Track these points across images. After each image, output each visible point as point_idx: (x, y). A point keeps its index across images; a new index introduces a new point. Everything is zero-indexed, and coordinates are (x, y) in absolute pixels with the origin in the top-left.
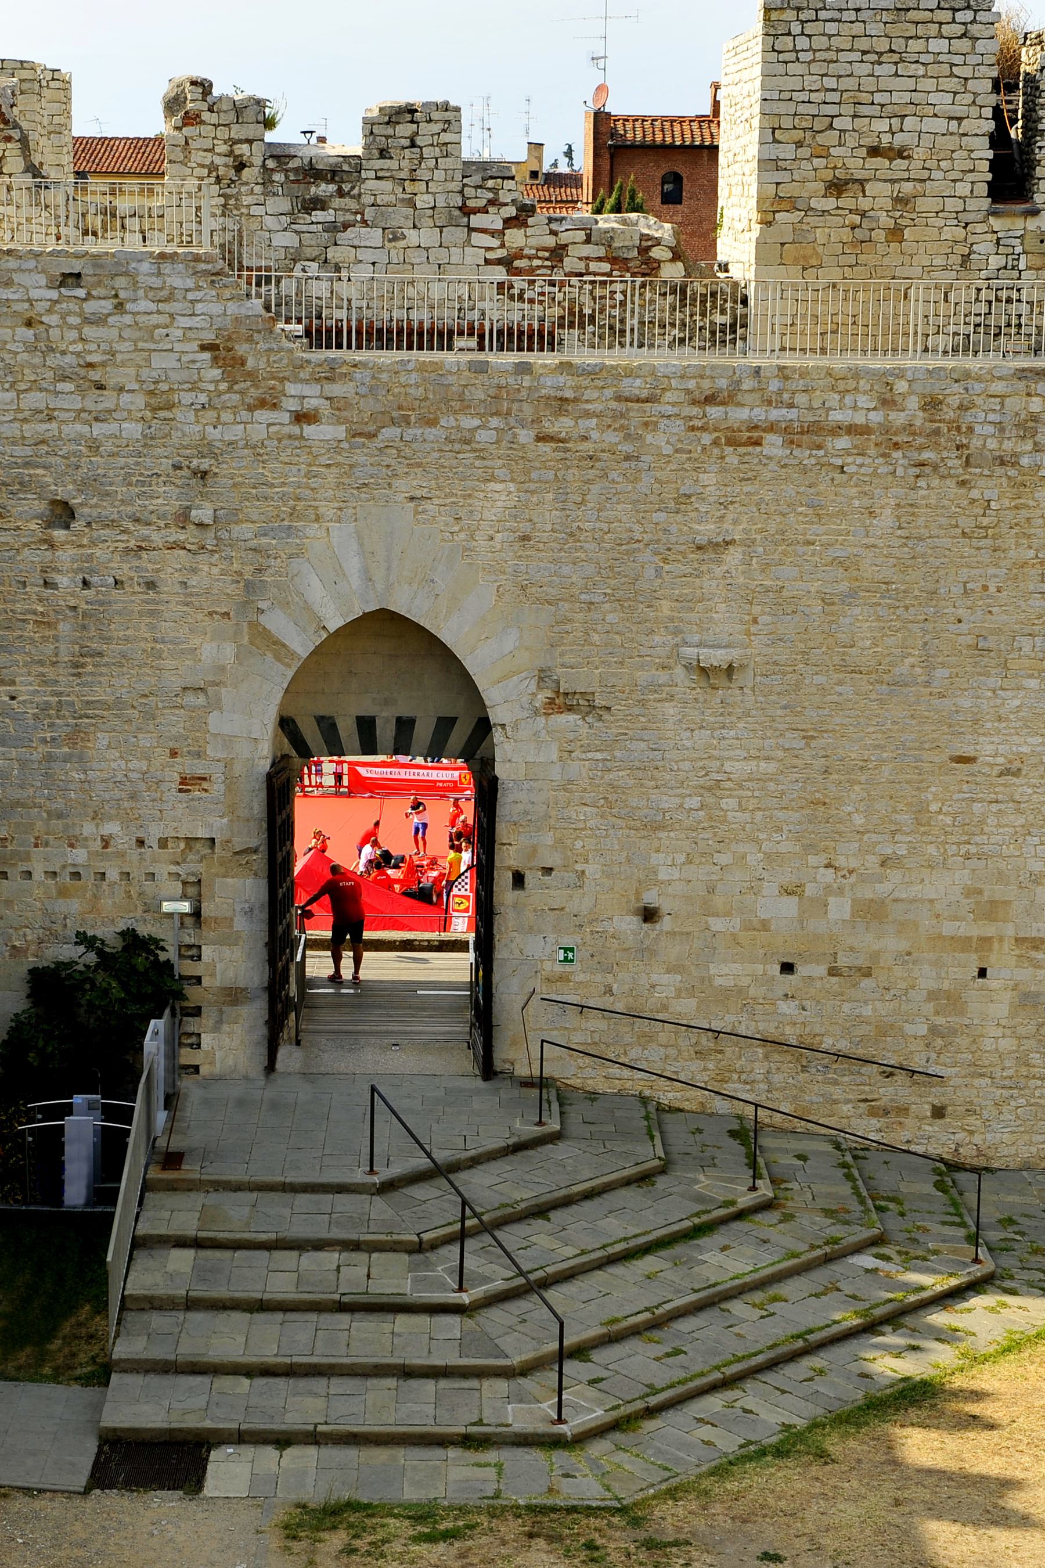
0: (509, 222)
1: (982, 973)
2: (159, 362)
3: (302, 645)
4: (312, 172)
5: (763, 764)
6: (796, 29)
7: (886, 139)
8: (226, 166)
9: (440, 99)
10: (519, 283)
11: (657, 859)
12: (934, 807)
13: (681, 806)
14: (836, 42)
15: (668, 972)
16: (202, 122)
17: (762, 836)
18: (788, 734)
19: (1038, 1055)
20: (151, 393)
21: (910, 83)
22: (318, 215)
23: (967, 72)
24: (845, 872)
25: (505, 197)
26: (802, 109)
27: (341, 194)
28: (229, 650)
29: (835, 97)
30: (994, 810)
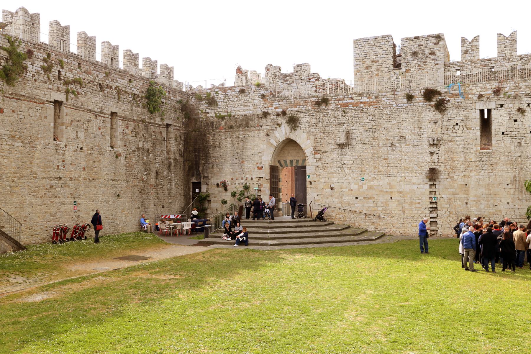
0: (316, 80)
4: (286, 76)
7: (375, 59)
10: (318, 90)
11: (333, 179)
12: (381, 168)
22: (287, 82)
25: (315, 76)
27: (290, 78)
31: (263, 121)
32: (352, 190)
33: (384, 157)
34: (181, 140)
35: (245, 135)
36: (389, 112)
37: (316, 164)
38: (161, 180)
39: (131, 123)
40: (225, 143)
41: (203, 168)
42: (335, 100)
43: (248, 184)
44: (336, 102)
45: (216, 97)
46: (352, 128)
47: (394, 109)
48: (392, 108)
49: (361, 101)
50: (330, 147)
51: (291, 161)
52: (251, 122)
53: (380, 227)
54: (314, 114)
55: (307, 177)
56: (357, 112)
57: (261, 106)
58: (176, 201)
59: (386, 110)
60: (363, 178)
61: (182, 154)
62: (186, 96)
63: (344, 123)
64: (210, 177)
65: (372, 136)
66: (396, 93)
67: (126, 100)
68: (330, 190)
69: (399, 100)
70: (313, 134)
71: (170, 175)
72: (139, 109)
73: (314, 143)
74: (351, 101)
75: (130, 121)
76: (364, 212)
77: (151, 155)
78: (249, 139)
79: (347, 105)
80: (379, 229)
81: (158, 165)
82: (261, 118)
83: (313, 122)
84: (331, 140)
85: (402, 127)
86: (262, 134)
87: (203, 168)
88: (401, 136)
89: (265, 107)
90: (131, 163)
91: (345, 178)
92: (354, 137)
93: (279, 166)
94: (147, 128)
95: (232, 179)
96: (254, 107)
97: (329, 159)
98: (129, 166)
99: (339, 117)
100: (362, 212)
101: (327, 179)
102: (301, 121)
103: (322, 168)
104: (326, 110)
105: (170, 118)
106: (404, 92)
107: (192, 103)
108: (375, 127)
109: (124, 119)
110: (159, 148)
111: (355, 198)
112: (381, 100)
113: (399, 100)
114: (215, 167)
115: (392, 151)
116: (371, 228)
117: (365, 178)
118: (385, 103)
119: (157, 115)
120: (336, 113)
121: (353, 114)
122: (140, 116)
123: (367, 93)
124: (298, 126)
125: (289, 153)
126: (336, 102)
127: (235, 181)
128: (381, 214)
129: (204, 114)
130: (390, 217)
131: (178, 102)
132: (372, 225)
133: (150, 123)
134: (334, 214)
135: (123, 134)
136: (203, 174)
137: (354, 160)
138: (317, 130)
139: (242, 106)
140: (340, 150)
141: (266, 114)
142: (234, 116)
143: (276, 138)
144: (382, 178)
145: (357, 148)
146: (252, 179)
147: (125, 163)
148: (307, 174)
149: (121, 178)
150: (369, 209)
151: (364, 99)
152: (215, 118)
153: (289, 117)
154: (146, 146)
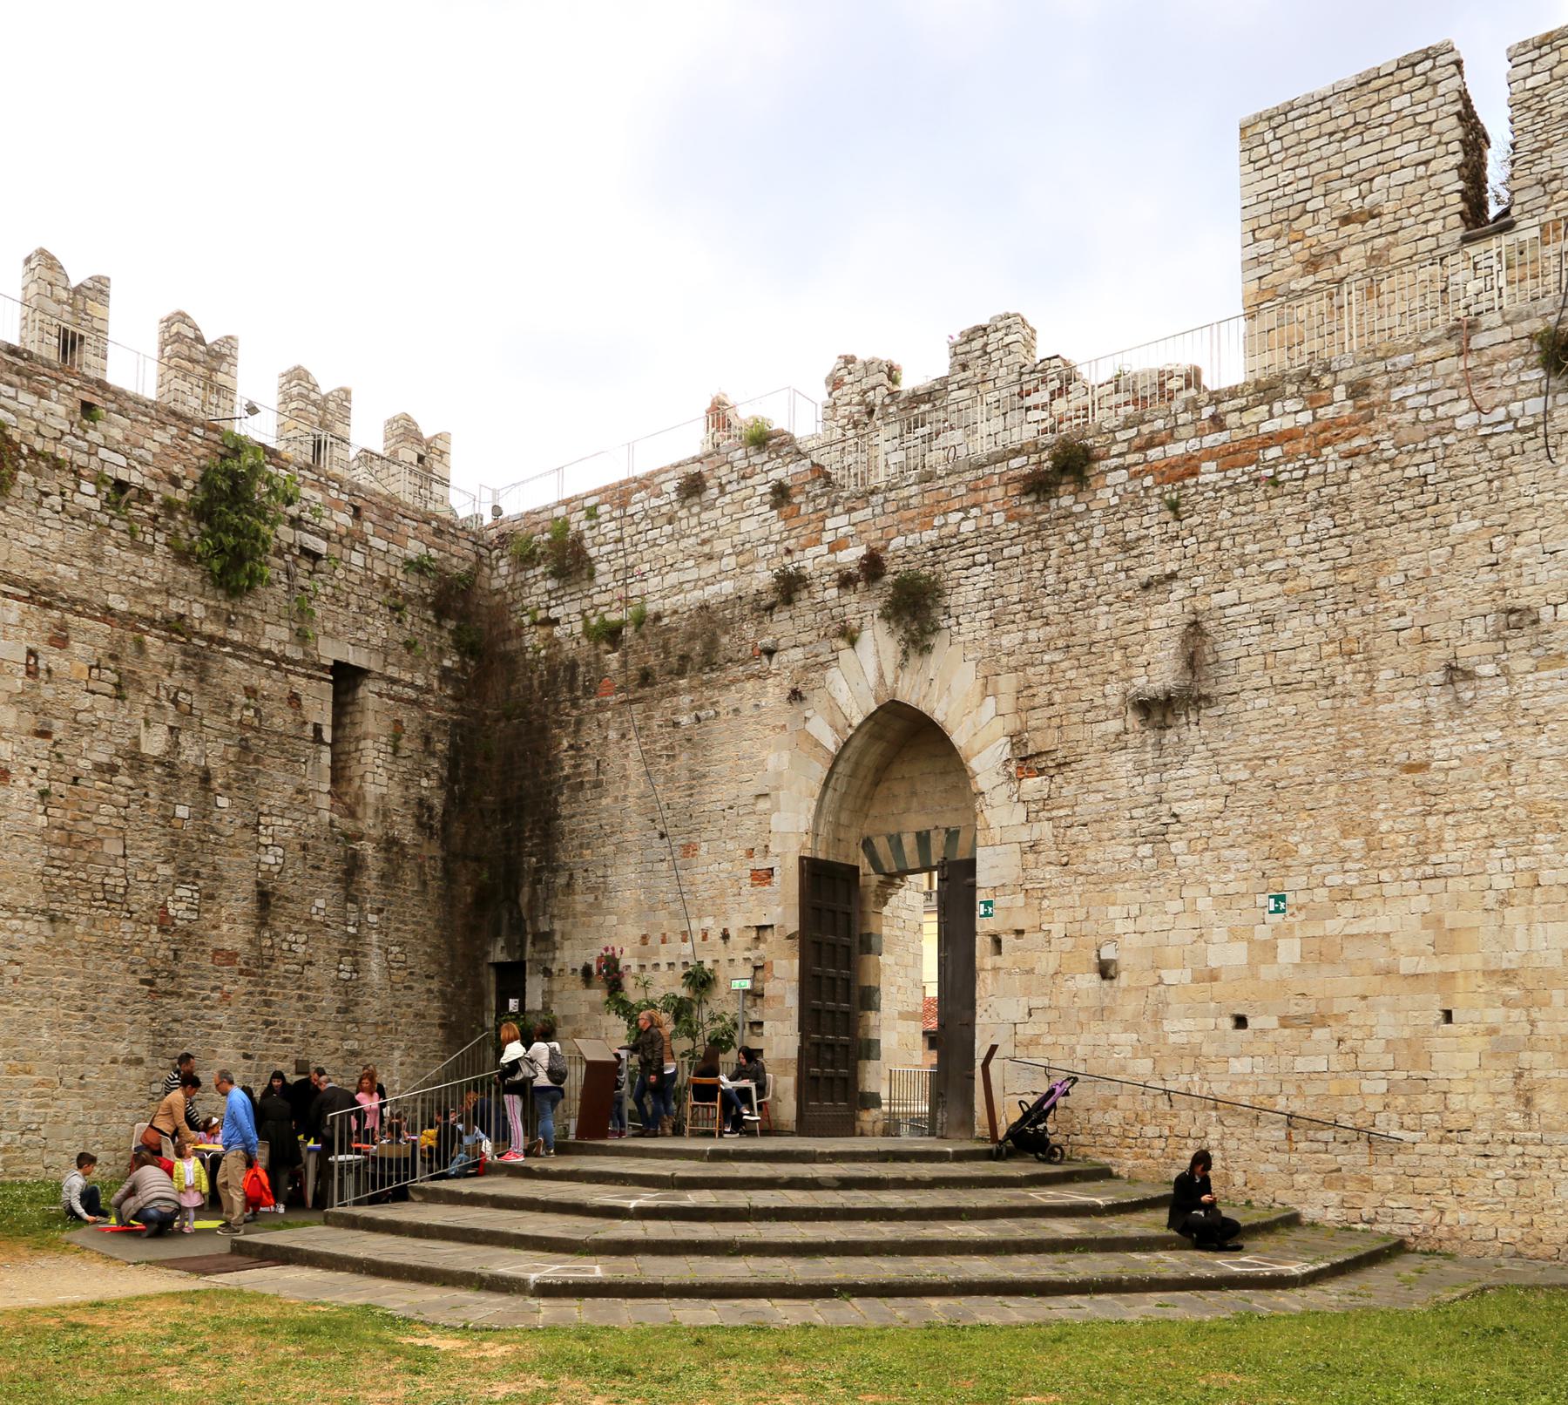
1: (1448, 1016)
3: (831, 742)
5: (1209, 801)
6: (1269, 136)
8: (859, 412)
9: (1002, 312)
11: (1114, 911)
12: (1384, 827)
13: (1135, 855)
14: (1305, 135)
15: (1126, 1031)
16: (844, 384)
17: (1211, 878)
18: (1233, 767)
20: (741, 553)
21: (1376, 146)
23: (1430, 116)
24: (1294, 909)
26: (1277, 204)
28: (786, 756)
29: (1307, 182)
30: (1451, 822)
31: (781, 626)
32: (1213, 977)
33: (1401, 757)
34: (433, 754)
35: (701, 707)
36: (1431, 468)
37: (1025, 835)
38: (291, 937)
39: (90, 623)
40: (619, 762)
41: (534, 891)
42: (1123, 447)
43: (708, 965)
44: (1131, 458)
45: (587, 534)
46: (1217, 599)
48: (1449, 439)
49: (1267, 427)
50: (1099, 729)
51: (923, 839)
52: (725, 640)
53: (1373, 1198)
54: (1017, 550)
55: (981, 909)
56: (1244, 496)
57: (772, 547)
58: (392, 1048)
59: (1418, 458)
60: (1280, 898)
61: (437, 824)
62: (469, 545)
63: (1172, 576)
64: (557, 938)
65: (1335, 632)
66: (1479, 341)
67: (56, 500)
68: (1096, 977)
69: (1496, 382)
71: (353, 917)
72: (147, 561)
73: (1018, 711)
74: (1208, 441)
75: (78, 614)
76: (1281, 1103)
77: (223, 802)
78: (718, 727)
79: (1188, 467)
80: (1367, 1213)
81: (271, 860)
82: (770, 608)
83: (1014, 591)
84: (1105, 682)
85: (1517, 552)
86: (773, 693)
87: (534, 891)
88: (1512, 611)
89: (789, 552)
90: (85, 826)
91: (1175, 906)
92: (1231, 649)
93: (864, 864)
94: (198, 664)
96: (741, 559)
97: (1093, 798)
98: (68, 842)
99: (1145, 546)
100: (1267, 1103)
101: (1081, 914)
102: (946, 601)
103: (1053, 855)
104: (1078, 516)
105: (360, 635)
106: (1525, 327)
107: (497, 584)
108: (1352, 574)
110: (280, 776)
111: (1228, 1023)
112: (1384, 405)
113: (1496, 382)
114: (579, 882)
115: (1452, 716)
116: (1321, 1206)
117: (1290, 897)
118: (1409, 416)
119: (271, 608)
120: (1130, 524)
121: (1224, 514)
122: (157, 600)
123: (1305, 376)
124: (937, 629)
125: (914, 794)
126: (1131, 458)
127: (657, 954)
128: (1381, 1120)
129: (543, 632)
130: (1435, 1135)
132: (1327, 1184)
133: (223, 642)
134: (1113, 1118)
135: (32, 672)
136: (534, 920)
137: (1226, 789)
138: (1032, 636)
139: (691, 563)
140: (1151, 736)
141: (790, 586)
142: (658, 617)
143: (834, 706)
144: (1391, 890)
145: (1246, 717)
146: (725, 936)
147: (41, 821)
148: (981, 896)
150: (1309, 1089)
151: (1289, 415)
152: (584, 642)
154: (190, 753)
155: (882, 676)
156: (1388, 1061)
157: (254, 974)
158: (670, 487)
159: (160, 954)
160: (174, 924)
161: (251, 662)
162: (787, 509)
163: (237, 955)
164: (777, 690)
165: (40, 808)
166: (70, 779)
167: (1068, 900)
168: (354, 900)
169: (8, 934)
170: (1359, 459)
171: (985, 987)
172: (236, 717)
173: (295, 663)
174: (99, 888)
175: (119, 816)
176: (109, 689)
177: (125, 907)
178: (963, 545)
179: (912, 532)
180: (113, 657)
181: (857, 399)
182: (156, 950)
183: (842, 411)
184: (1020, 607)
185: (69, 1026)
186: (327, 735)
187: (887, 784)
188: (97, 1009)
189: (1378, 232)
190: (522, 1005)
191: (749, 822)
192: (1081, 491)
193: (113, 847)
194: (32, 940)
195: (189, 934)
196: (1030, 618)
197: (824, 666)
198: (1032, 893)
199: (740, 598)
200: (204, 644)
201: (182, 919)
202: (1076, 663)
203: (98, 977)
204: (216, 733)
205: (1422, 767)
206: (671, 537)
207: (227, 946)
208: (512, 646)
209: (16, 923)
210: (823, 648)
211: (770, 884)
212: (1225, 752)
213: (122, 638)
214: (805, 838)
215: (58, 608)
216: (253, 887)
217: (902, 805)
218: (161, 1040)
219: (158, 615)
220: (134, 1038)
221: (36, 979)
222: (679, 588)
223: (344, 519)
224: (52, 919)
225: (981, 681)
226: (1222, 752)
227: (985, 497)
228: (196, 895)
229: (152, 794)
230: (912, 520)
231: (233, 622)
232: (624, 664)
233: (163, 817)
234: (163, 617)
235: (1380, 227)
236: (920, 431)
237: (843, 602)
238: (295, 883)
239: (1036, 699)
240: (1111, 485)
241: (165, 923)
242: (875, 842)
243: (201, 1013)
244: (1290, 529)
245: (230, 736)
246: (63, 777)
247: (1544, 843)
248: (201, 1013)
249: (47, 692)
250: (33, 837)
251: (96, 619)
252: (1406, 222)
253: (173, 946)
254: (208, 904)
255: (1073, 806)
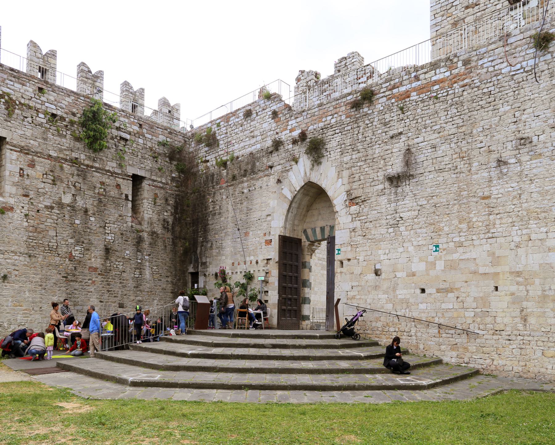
2: (265, 125)
3: (290, 196)
5: (413, 212)
8: (306, 89)
9: (351, 52)
11: (380, 252)
12: (474, 220)
13: (387, 232)
15: (384, 294)
16: (301, 80)
17: (413, 240)
18: (421, 200)
19: (521, 325)
20: (263, 135)
24: (442, 250)
26: (443, 5)
30: (498, 217)
31: (275, 158)
32: (414, 275)
33: (481, 194)
34: (169, 205)
35: (250, 187)
36: (492, 88)
37: (351, 226)
38: (117, 263)
40: (226, 206)
41: (201, 249)
42: (384, 90)
43: (252, 272)
44: (387, 93)
45: (217, 132)
46: (416, 140)
47: (506, 79)
48: (499, 78)
49: (434, 78)
51: (322, 229)
52: (258, 164)
53: (468, 355)
54: (349, 128)
55: (336, 252)
56: (426, 104)
57: (272, 132)
58: (154, 300)
59: (488, 85)
60: (437, 246)
61: (170, 227)
62: (181, 137)
63: (401, 133)
64: (208, 264)
65: (458, 150)
66: (511, 40)
68: (374, 275)
69: (517, 55)
70: (347, 166)
71: (140, 257)
73: (349, 183)
74: (414, 85)
76: (436, 320)
77: (92, 219)
78: (255, 193)
79: (407, 95)
80: (466, 360)
81: (110, 238)
82: (271, 152)
83: (348, 142)
84: (378, 171)
85: (524, 117)
86: (272, 180)
87: (201, 249)
88: (522, 139)
90: (41, 226)
91: (401, 250)
92: (421, 158)
93: (304, 239)
95: (233, 263)
96: (263, 137)
97: (374, 212)
99: (392, 123)
100: (432, 320)
101: (369, 253)
102: (327, 146)
103: (360, 233)
105: (142, 165)
106: (529, 33)
107: (191, 150)
108: (464, 129)
109: (24, 150)
110: (113, 211)
111: (419, 291)
112: (476, 67)
113: (517, 55)
114: (214, 246)
115: (499, 178)
116: (450, 357)
117: (441, 246)
118: (485, 70)
119: (110, 156)
120: (387, 116)
121: (419, 110)
122: (67, 153)
123: (448, 59)
124: (323, 156)
125: (320, 214)
126: (387, 93)
127: (237, 268)
128: (472, 327)
129: (205, 165)
130: (491, 332)
131: (160, 144)
132: (452, 349)
133: (92, 167)
134: (379, 324)
136: (201, 258)
137: (419, 208)
138: (354, 157)
139: (248, 139)
140: (393, 190)
141: (277, 145)
142: (238, 158)
143: (291, 184)
144: (476, 243)
145: (425, 182)
146: (257, 263)
147: (26, 224)
148: (337, 247)
149: (13, 249)
150: (446, 315)
151: (442, 73)
152: (216, 167)
153: (310, 142)
154: (80, 203)
155: (306, 173)
156: (474, 305)
157: (104, 275)
158: (241, 115)
159: (69, 268)
160: (74, 258)
161: (102, 174)
162: (277, 119)
163: (97, 269)
164: (273, 180)
165: (25, 220)
166: (36, 211)
167: (365, 248)
168: (140, 251)
169: (13, 261)
170: (466, 87)
171: (338, 279)
172: (97, 191)
173: (118, 174)
174: (47, 246)
175: (54, 223)
176: (50, 181)
177: (57, 252)
178: (332, 127)
179: (315, 124)
180: (52, 171)
181: (305, 84)
182: (68, 267)
183: (301, 89)
184: (350, 147)
185: (36, 291)
186: (130, 198)
187: (311, 211)
188: (46, 285)
189: (478, 10)
190: (198, 286)
191: (265, 224)
192: (371, 106)
193: (52, 233)
194: (22, 263)
195: (80, 262)
196: (353, 151)
197: (288, 171)
198: (353, 246)
199: (262, 150)
200: (85, 167)
201: (77, 257)
202: (368, 165)
203: (47, 275)
204: (90, 196)
205: (488, 197)
206: (242, 131)
207: (94, 265)
208: (195, 170)
209: (16, 257)
210: (287, 165)
211: (271, 245)
212: (418, 194)
213: (55, 165)
214: (282, 229)
215: (31, 155)
216: (103, 247)
217: (316, 218)
218: (70, 296)
219: (68, 158)
220: (60, 295)
221: (24, 276)
222: (244, 148)
223: (136, 128)
224: (30, 256)
225: (337, 173)
226: (417, 194)
227: (339, 110)
228: (83, 249)
229: (66, 216)
230: (315, 120)
231: (96, 161)
232: (227, 173)
233: (71, 223)
234: (70, 159)
235: (479, 9)
236: (325, 94)
237: (294, 149)
238: (118, 246)
239: (355, 179)
240: (380, 103)
241: (71, 258)
242: (307, 231)
243: (84, 287)
244: (442, 114)
245: (95, 197)
246: (33, 210)
247: (533, 224)
248: (84, 287)
249: (27, 182)
250: (22, 229)
251: (45, 158)
252: (488, 6)
253: (74, 266)
254: (87, 252)
255: (367, 215)
